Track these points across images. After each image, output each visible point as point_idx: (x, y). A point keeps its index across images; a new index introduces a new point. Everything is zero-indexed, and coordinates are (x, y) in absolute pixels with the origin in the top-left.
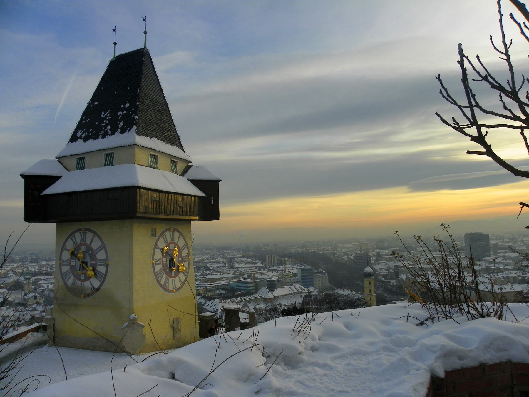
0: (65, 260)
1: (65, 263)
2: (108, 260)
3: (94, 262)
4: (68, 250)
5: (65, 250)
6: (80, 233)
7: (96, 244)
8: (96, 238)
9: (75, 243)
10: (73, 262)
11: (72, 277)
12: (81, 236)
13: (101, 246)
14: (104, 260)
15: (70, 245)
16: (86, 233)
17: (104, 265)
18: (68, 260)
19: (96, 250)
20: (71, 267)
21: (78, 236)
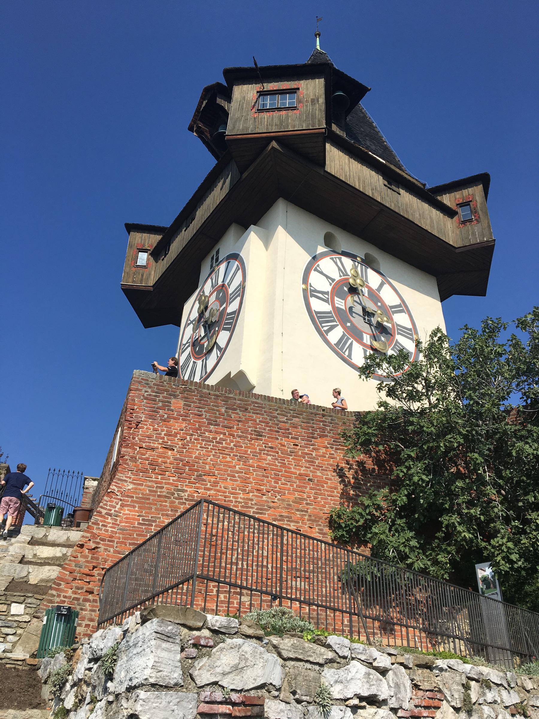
0: (318, 289)
5: (316, 270)
7: (389, 297)
8: (386, 287)
9: (342, 270)
10: (339, 303)
13: (399, 306)
14: (410, 330)
18: (327, 293)
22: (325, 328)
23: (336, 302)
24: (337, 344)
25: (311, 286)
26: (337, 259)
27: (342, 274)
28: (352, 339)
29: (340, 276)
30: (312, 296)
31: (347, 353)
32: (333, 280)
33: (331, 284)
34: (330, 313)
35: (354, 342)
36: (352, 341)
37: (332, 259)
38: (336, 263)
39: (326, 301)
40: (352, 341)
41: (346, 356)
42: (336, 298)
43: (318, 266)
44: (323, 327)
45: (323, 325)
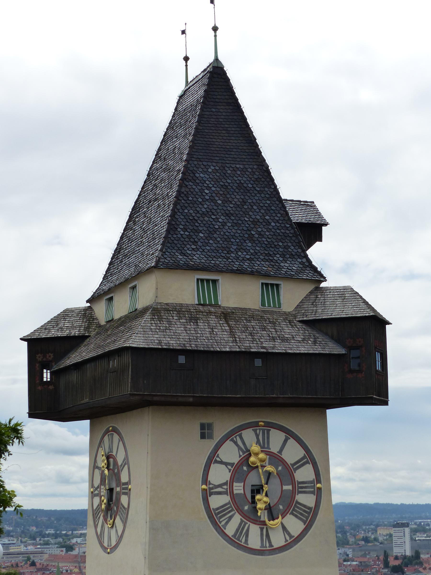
1: (219, 489)
2: (319, 481)
3: (290, 487)
4: (226, 464)
5: (216, 462)
6: (255, 431)
7: (292, 453)
8: (291, 441)
10: (238, 488)
11: (237, 519)
12: (257, 436)
13: (304, 457)
15: (230, 453)
16: (268, 431)
17: (313, 493)
18: (226, 484)
19: (293, 465)
20: (233, 496)
21: (249, 436)
22: (223, 523)
23: (234, 488)
24: (234, 536)
25: (210, 484)
26: (238, 437)
27: (241, 453)
28: (249, 523)
29: (240, 456)
30: (211, 494)
31: (243, 540)
32: (232, 464)
33: (230, 470)
34: (229, 503)
35: (251, 524)
36: (249, 525)
37: (232, 440)
38: (236, 443)
39: (226, 493)
40: (249, 525)
41: (242, 544)
42: (235, 484)
43: (218, 456)
44: (220, 522)
45: (221, 520)
